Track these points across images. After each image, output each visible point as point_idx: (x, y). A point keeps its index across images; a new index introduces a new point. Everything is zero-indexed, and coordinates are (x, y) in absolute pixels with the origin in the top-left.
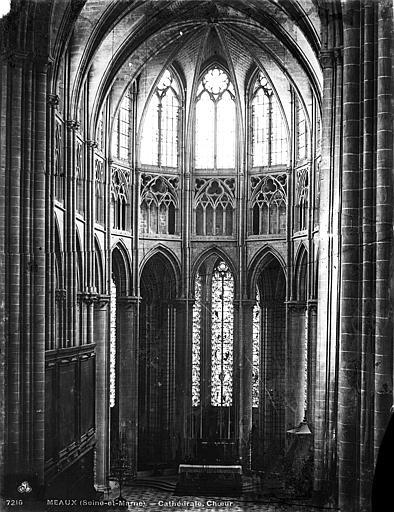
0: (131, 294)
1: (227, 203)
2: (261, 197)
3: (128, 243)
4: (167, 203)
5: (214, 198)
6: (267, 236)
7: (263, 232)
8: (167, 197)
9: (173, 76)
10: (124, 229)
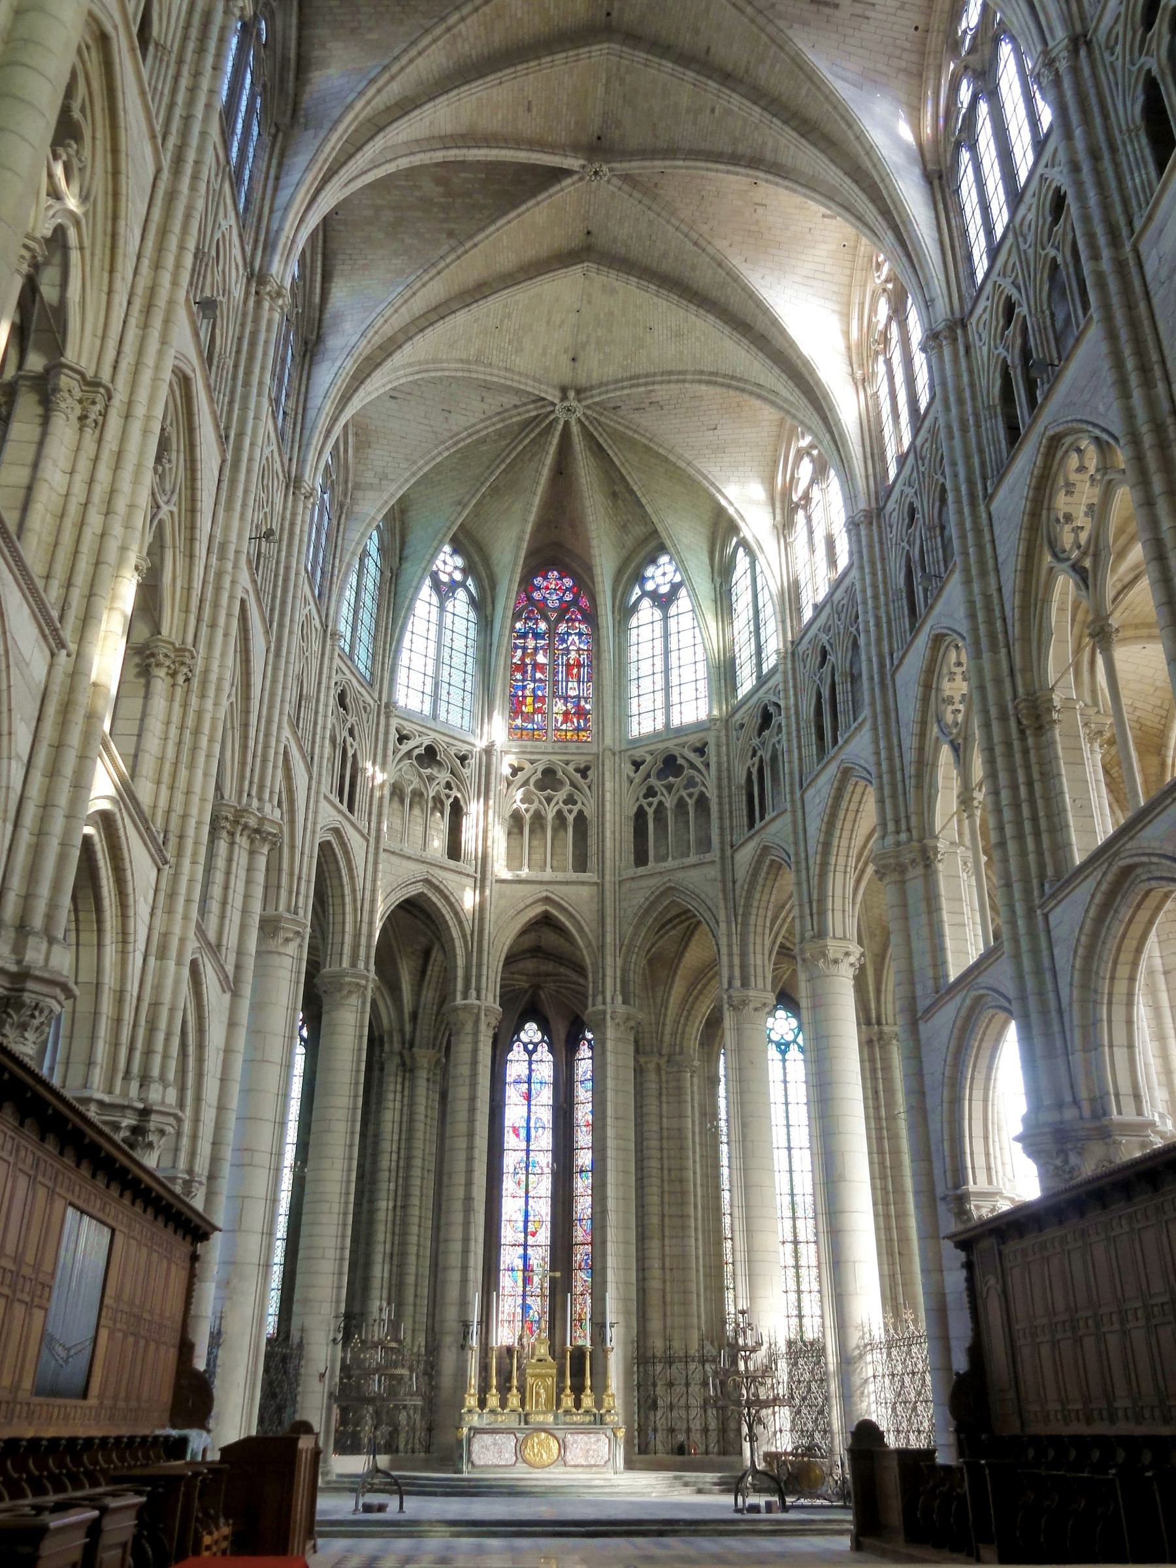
0: (354, 964)
1: (576, 809)
2: (651, 792)
4: (448, 797)
6: (670, 863)
8: (448, 786)
9: (464, 571)
10: (351, 808)
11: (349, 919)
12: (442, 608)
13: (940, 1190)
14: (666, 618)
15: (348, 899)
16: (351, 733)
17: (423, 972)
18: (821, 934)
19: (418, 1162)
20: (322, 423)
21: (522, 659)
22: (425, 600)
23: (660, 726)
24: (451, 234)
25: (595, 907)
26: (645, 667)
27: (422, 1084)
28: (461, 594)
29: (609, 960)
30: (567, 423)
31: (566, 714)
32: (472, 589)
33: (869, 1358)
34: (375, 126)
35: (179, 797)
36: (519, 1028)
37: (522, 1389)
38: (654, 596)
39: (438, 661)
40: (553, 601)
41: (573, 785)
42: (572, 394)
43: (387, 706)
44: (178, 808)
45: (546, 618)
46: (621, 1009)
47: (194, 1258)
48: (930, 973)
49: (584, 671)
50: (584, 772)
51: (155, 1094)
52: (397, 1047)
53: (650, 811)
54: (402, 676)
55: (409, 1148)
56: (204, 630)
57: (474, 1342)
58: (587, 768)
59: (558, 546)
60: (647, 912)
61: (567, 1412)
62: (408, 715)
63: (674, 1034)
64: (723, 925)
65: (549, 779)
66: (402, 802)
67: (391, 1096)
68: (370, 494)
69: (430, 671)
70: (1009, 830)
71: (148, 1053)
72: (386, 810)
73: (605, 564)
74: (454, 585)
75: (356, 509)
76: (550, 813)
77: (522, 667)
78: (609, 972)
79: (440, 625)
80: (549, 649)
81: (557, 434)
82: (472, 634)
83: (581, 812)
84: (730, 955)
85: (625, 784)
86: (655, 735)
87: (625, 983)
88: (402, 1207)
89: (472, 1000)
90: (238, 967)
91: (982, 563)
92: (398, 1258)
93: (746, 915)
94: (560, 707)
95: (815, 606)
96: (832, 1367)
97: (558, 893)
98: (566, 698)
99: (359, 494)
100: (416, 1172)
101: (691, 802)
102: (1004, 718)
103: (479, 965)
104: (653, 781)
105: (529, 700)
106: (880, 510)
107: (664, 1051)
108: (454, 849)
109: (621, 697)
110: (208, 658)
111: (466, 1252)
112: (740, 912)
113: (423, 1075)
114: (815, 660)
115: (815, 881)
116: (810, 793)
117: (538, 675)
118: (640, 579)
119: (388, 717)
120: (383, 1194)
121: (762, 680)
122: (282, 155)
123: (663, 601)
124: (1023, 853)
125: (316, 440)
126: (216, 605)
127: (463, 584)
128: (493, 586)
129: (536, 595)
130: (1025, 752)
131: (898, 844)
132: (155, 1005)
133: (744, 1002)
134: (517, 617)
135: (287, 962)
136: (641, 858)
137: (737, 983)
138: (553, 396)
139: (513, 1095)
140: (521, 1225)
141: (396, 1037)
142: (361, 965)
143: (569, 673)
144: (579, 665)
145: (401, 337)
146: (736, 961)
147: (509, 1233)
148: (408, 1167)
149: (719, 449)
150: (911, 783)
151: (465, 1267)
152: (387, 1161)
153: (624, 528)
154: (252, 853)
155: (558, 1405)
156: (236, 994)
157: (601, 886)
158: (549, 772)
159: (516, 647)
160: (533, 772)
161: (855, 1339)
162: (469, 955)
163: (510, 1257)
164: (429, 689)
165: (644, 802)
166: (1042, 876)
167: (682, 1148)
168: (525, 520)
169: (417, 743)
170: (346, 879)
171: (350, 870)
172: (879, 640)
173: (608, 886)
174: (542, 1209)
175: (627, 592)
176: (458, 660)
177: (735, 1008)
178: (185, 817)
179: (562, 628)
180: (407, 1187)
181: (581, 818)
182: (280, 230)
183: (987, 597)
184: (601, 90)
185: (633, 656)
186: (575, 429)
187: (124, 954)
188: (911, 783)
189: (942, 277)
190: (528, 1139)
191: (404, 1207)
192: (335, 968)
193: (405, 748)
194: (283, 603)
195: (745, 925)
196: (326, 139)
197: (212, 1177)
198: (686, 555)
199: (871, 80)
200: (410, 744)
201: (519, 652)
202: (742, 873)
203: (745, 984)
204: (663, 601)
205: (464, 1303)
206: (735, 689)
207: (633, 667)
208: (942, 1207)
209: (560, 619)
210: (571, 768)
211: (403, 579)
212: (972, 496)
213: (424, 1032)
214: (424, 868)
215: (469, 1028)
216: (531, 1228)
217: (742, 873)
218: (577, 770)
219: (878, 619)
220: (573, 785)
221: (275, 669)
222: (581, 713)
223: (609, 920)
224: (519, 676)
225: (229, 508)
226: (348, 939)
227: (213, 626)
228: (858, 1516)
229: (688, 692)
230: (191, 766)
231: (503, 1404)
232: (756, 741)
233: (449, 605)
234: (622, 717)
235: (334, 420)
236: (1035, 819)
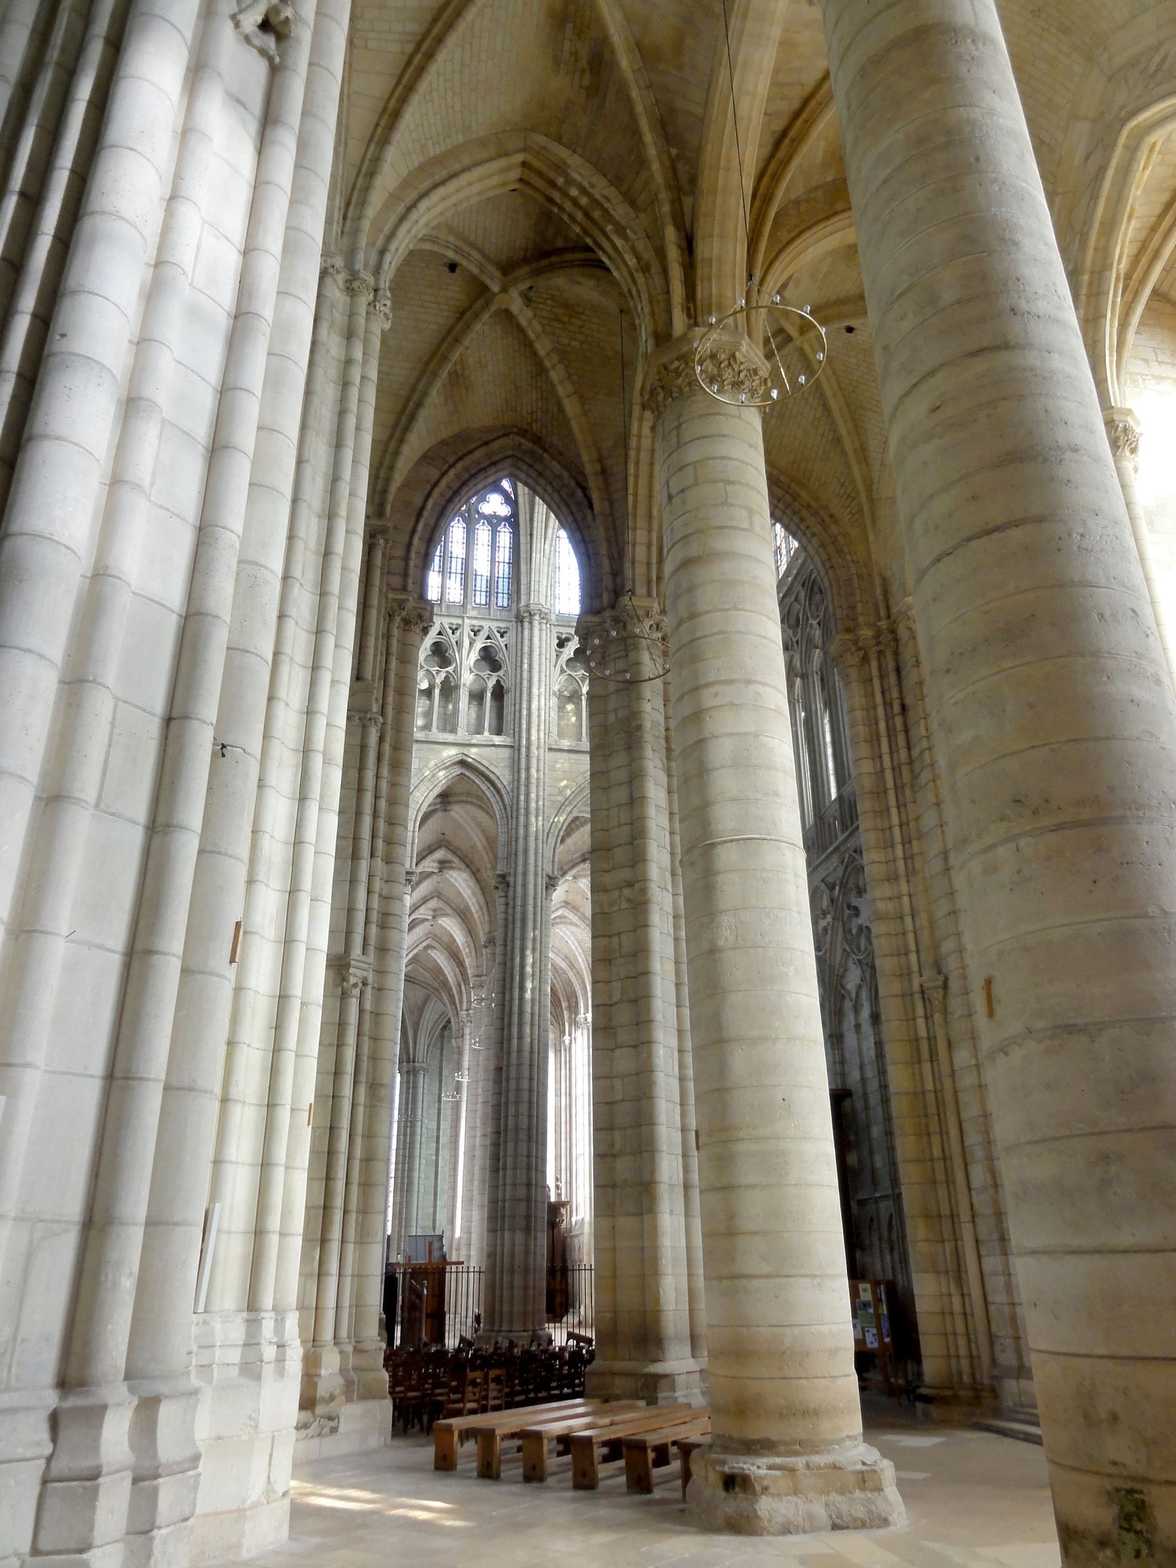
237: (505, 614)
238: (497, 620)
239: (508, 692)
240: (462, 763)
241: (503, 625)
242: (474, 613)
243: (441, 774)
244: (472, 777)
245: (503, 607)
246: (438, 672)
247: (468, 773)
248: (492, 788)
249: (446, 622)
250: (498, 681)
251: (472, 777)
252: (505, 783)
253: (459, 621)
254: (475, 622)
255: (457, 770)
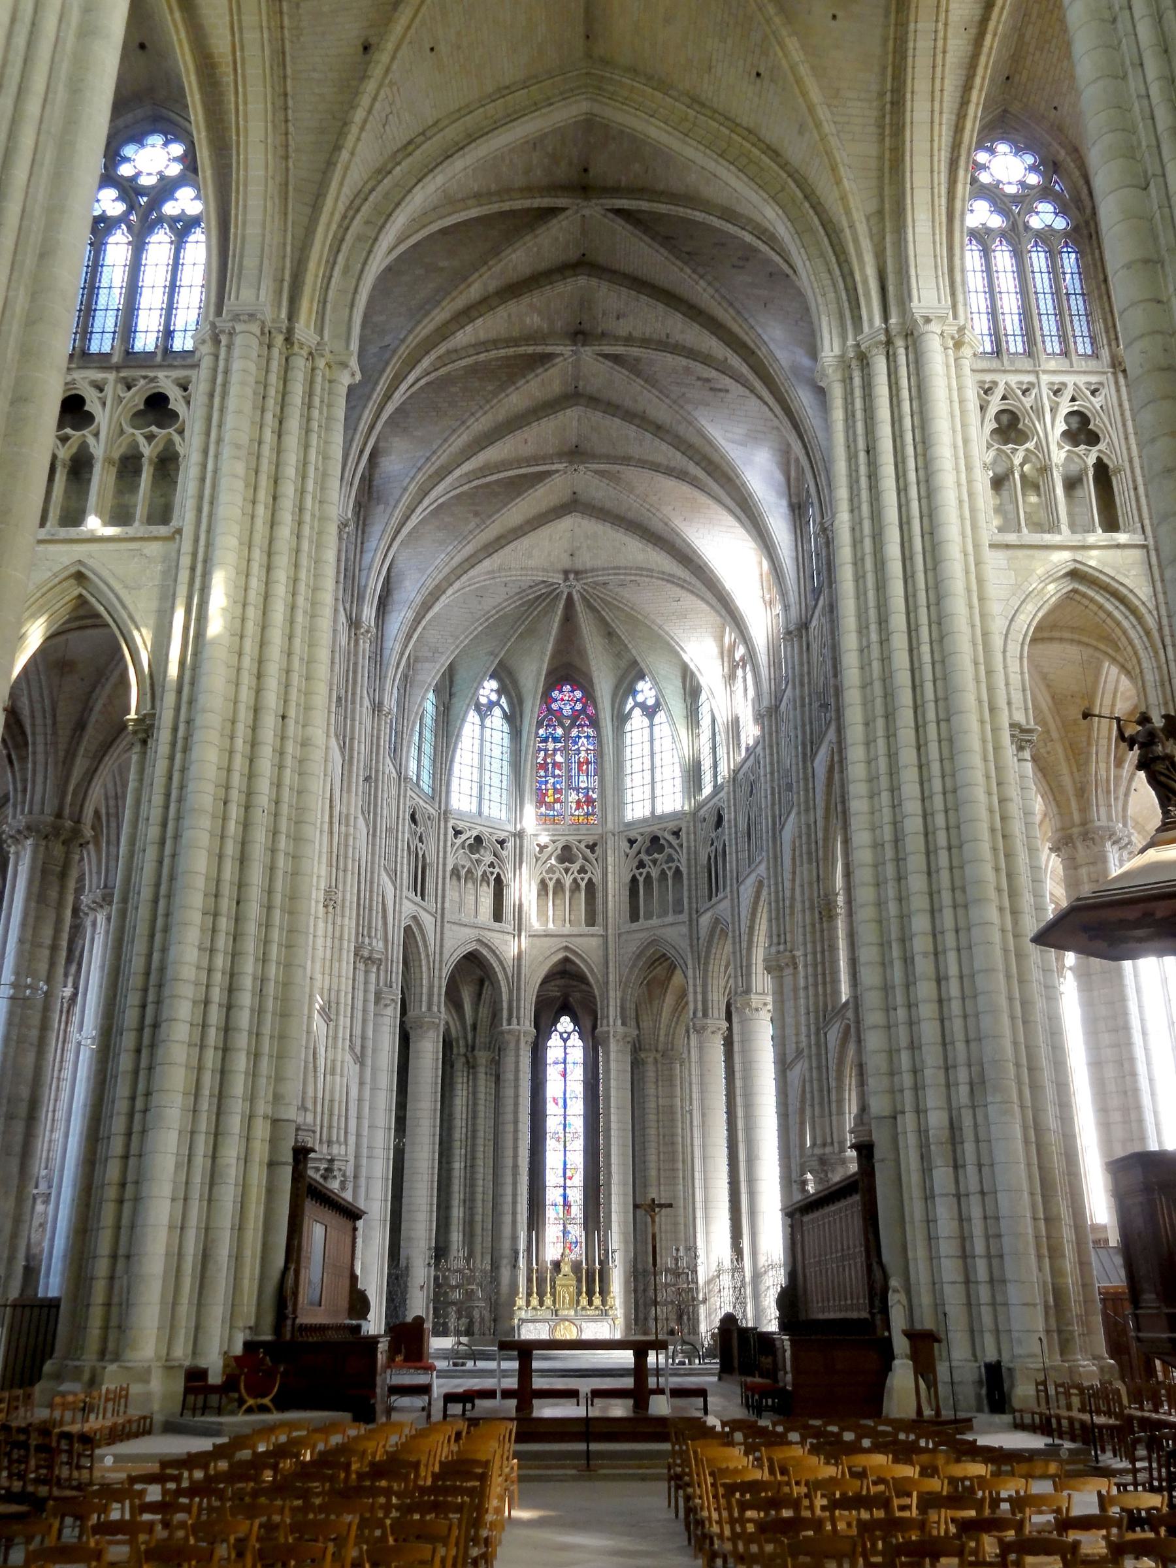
0: (429, 1008)
1: (587, 877)
2: (641, 865)
3: (428, 921)
5: (567, 870)
6: (654, 921)
7: (649, 916)
8: (492, 865)
9: (499, 692)
10: (423, 899)
11: (425, 975)
12: (483, 726)
13: (794, 1176)
14: (651, 726)
15: (424, 963)
16: (421, 840)
17: (480, 995)
18: (748, 991)
19: (481, 1134)
20: (393, 661)
21: (544, 759)
22: (471, 725)
23: (648, 813)
24: (476, 514)
25: (601, 953)
26: (637, 765)
27: (482, 1076)
28: (497, 711)
29: (612, 994)
30: (570, 596)
31: (578, 802)
32: (505, 706)
33: (770, 1273)
34: (424, 493)
35: (335, 980)
36: (556, 1021)
37: (553, 1294)
38: (643, 706)
39: (481, 768)
40: (567, 711)
41: (585, 859)
42: (572, 576)
43: (445, 812)
44: (335, 987)
45: (562, 725)
46: (620, 1029)
47: (355, 1229)
48: (794, 1039)
49: (592, 767)
50: (592, 847)
51: (335, 1150)
52: (462, 1050)
53: (641, 879)
54: (455, 782)
55: (474, 1125)
56: (341, 874)
57: (522, 1263)
58: (595, 845)
59: (569, 666)
60: (639, 956)
61: (583, 1308)
62: (461, 816)
63: (667, 1035)
64: (690, 973)
65: (566, 855)
66: (459, 879)
67: (459, 1086)
68: (427, 665)
69: (476, 777)
70: (811, 980)
71: (330, 1127)
72: (448, 886)
73: (604, 687)
74: (491, 705)
75: (419, 677)
76: (568, 881)
77: (544, 766)
78: (612, 1002)
79: (482, 740)
80: (566, 748)
81: (563, 602)
82: (506, 742)
83: (590, 880)
84: (695, 993)
85: (623, 858)
86: (644, 820)
87: (623, 1008)
88: (471, 1167)
89: (514, 1026)
90: (363, 1047)
91: (807, 802)
92: (469, 1202)
93: (706, 964)
94: (573, 796)
95: (747, 749)
96: (748, 1279)
97: (575, 943)
98: (578, 790)
99: (419, 666)
100: (480, 1141)
101: (670, 874)
102: (812, 908)
103: (519, 1000)
104: (643, 856)
105: (550, 792)
106: (777, 707)
107: (660, 1047)
108: (498, 916)
109: (619, 789)
110: (344, 891)
111: (515, 1203)
112: (703, 960)
113: (482, 1070)
114: (746, 789)
115: (744, 952)
116: (742, 888)
117: (557, 772)
118: (634, 692)
119: (446, 822)
120: (457, 1158)
121: (717, 789)
122: (364, 525)
123: (650, 712)
124: (816, 995)
125: (391, 674)
126: (346, 857)
127: (498, 703)
128: (521, 702)
129: (554, 706)
130: (822, 931)
131: (778, 952)
132: (332, 1101)
133: (704, 1028)
134: (540, 724)
135: (387, 1020)
136: (634, 916)
137: (700, 1014)
138: (558, 578)
139: (553, 1074)
140: (561, 1173)
141: (462, 1043)
142: (435, 1009)
143: (579, 769)
144: (588, 763)
145: (445, 584)
146: (700, 997)
147: (552, 1177)
148: (474, 1137)
149: (683, 616)
150: (787, 911)
151: (514, 1214)
152: (459, 1134)
153: (618, 655)
154: (367, 972)
155: (578, 1302)
156: (362, 1064)
157: (605, 938)
158: (566, 848)
159: (540, 750)
160: (555, 849)
161: (762, 1261)
162: (511, 992)
163: (553, 1195)
164: (475, 792)
165: (637, 872)
166: (825, 1011)
167: (673, 1120)
168: (542, 660)
169: (468, 835)
170: (422, 949)
171: (425, 941)
172: (773, 804)
173: (610, 938)
174: (577, 1159)
175: (623, 703)
176: (496, 765)
177: (697, 1031)
178: (338, 991)
179: (574, 732)
180: (473, 1151)
181: (590, 884)
182: (366, 586)
183: (808, 826)
184: (575, 423)
185: (628, 755)
186: (576, 597)
187: (315, 1077)
188: (787, 911)
189: (796, 588)
190: (565, 1106)
191: (472, 1166)
192: (417, 1012)
193: (459, 841)
194: (376, 797)
195: (706, 971)
196: (391, 515)
197: (356, 1177)
198: (663, 685)
199: (753, 438)
200: (463, 837)
201: (542, 754)
202: (703, 933)
203: (705, 1015)
204: (650, 712)
205: (514, 1238)
206: (700, 790)
207: (628, 764)
208: (795, 1187)
209: (573, 725)
210: (582, 846)
211: (454, 711)
212: (804, 754)
213: (482, 1039)
214: (476, 931)
215: (512, 1045)
216: (569, 1174)
217: (703, 933)
218: (587, 847)
219: (773, 788)
220: (585, 859)
221: (374, 845)
222: (590, 801)
223: (611, 964)
224: (542, 773)
225: (349, 791)
226: (425, 990)
227: (345, 871)
228: (722, 1364)
229: (668, 785)
230: (340, 960)
231: (541, 1303)
232: (713, 835)
233: (488, 722)
234: (620, 805)
235: (402, 654)
236: (824, 974)
237: (1092, 364)
238: (1085, 372)
239: (1118, 470)
240: (1074, 574)
241: (1094, 379)
242: (1052, 365)
243: (1051, 588)
244: (1091, 593)
245: (1085, 355)
246: (1014, 451)
247: (1083, 588)
248: (1122, 608)
249: (1013, 379)
250: (1099, 459)
251: (1091, 593)
252: (1144, 599)
253: (1031, 378)
254: (1057, 379)
255: (1068, 586)
